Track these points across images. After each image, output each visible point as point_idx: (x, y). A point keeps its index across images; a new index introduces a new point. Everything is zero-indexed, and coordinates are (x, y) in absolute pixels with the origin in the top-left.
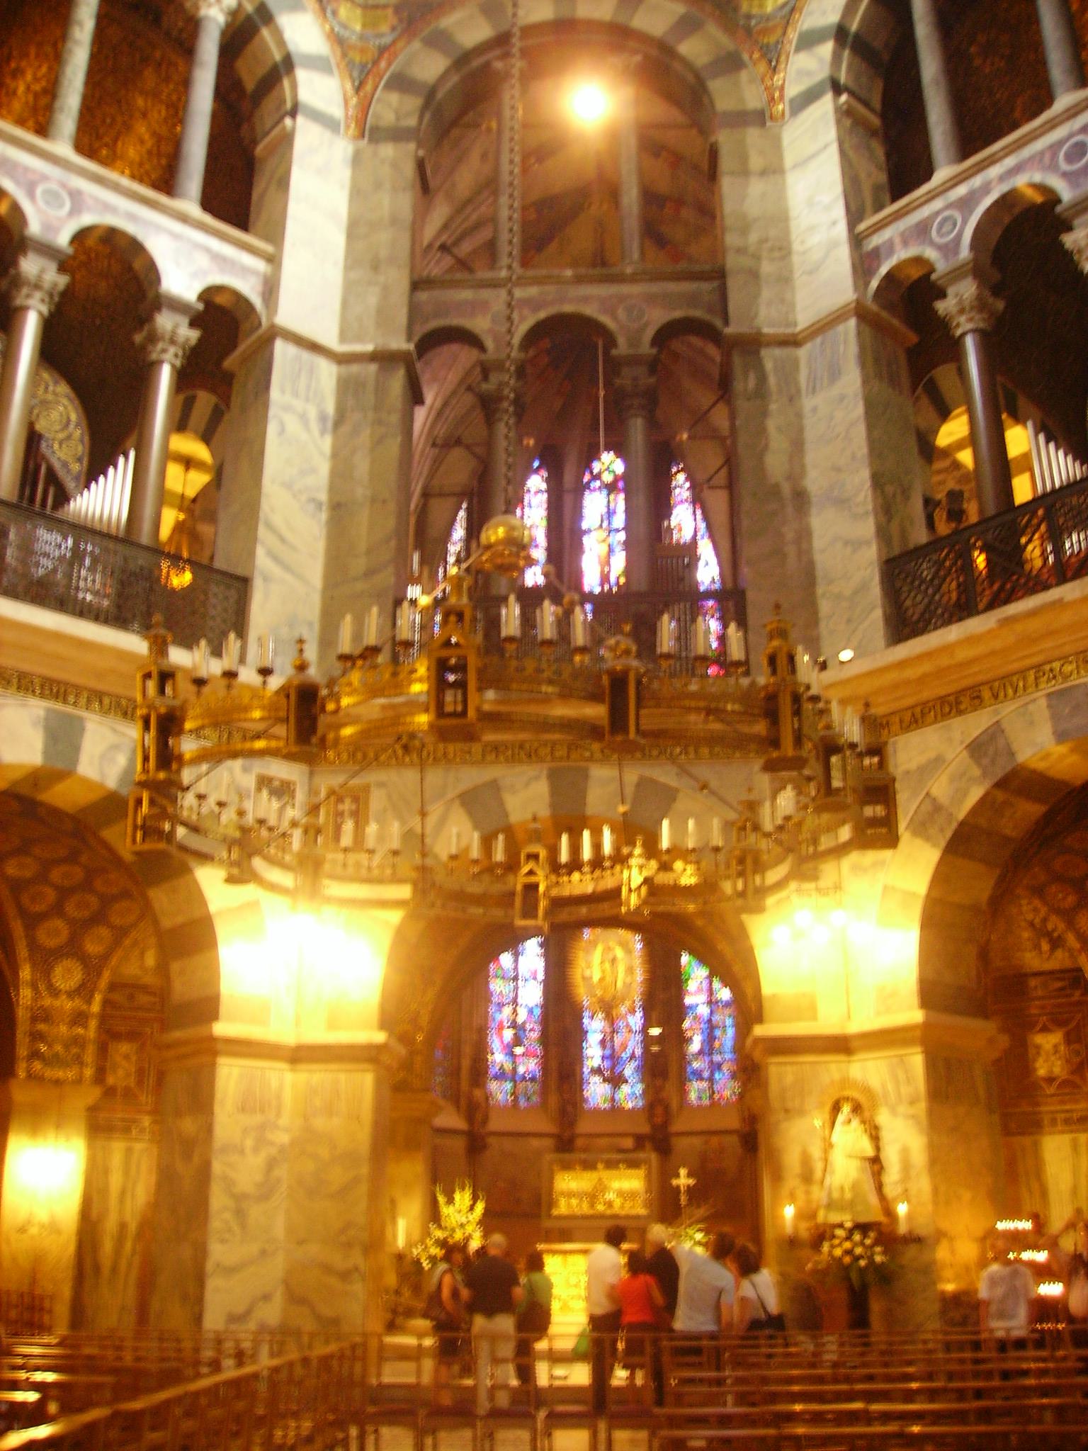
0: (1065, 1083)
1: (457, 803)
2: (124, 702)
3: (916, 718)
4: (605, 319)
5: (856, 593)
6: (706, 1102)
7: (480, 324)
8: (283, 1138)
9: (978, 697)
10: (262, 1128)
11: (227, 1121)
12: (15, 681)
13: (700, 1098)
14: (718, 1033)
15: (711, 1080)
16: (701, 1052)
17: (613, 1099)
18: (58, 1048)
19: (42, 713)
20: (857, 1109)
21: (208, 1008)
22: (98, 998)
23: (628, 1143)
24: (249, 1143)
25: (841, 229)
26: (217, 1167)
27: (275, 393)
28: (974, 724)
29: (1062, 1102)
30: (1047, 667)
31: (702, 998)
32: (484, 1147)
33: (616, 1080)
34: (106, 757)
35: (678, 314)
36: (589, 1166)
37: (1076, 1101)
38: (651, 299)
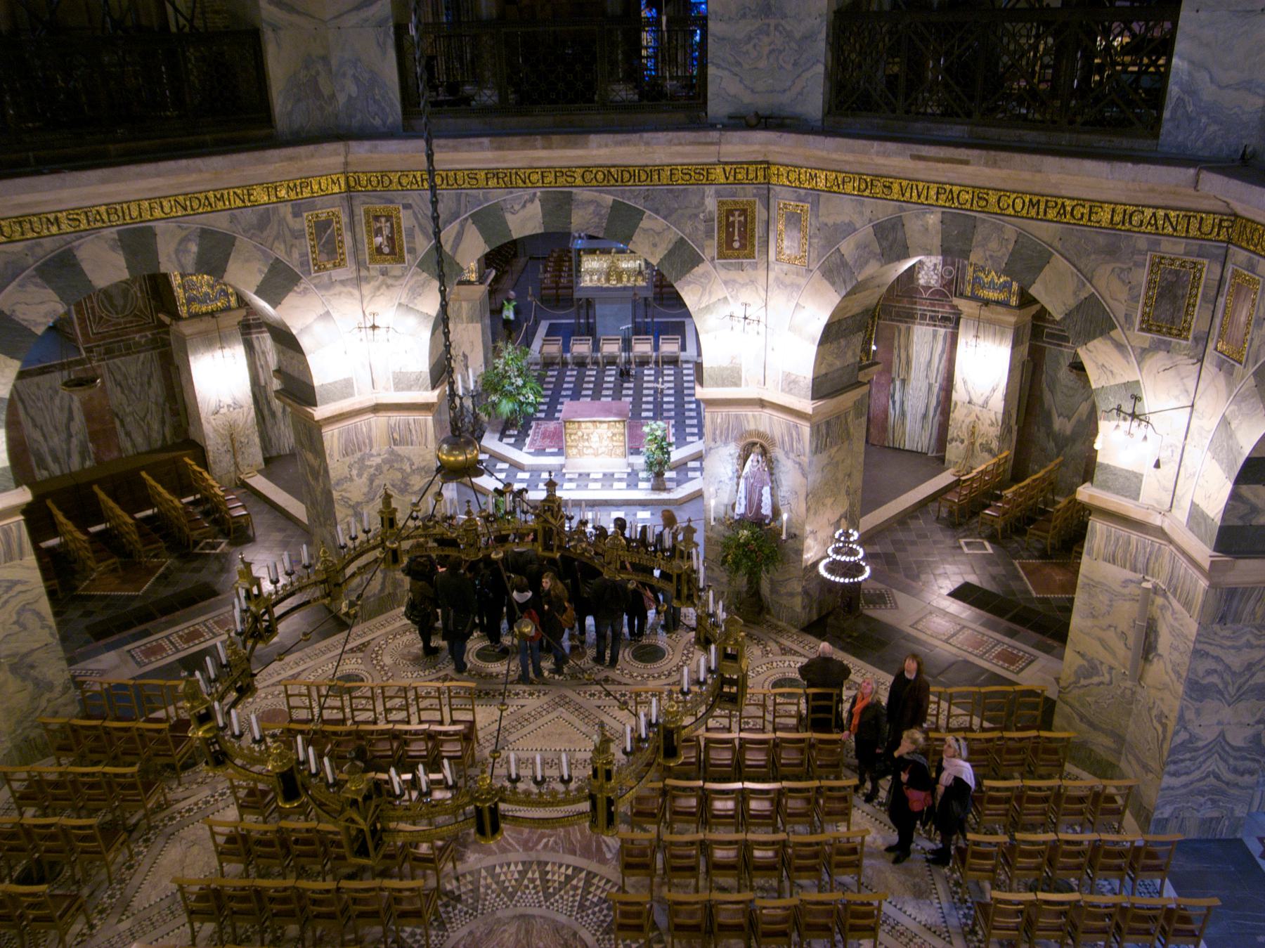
0: (937, 292)
1: (470, 221)
2: (181, 199)
5: (805, 38)
8: (378, 460)
9: (889, 187)
10: (362, 460)
11: (336, 464)
12: (83, 217)
18: (205, 289)
20: (764, 452)
24: (354, 472)
26: (336, 495)
29: (933, 305)
30: (948, 187)
34: (180, 250)
36: (606, 252)
37: (943, 306)
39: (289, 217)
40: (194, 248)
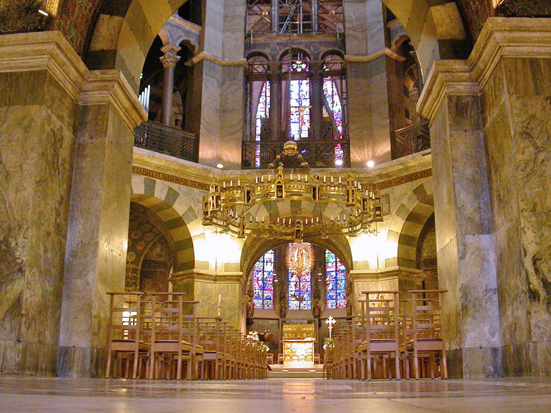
3: (400, 181)
4: (306, 50)
6: (334, 307)
7: (267, 51)
12: (136, 170)
13: (332, 306)
14: (339, 282)
15: (336, 299)
16: (332, 289)
17: (300, 307)
19: (143, 179)
21: (191, 264)
22: (140, 264)
23: (306, 322)
25: (382, 25)
27: (204, 76)
28: (416, 183)
31: (334, 269)
32: (252, 323)
33: (301, 300)
35: (330, 49)
38: (321, 43)
39: (197, 194)
40: (166, 191)
